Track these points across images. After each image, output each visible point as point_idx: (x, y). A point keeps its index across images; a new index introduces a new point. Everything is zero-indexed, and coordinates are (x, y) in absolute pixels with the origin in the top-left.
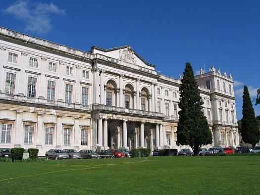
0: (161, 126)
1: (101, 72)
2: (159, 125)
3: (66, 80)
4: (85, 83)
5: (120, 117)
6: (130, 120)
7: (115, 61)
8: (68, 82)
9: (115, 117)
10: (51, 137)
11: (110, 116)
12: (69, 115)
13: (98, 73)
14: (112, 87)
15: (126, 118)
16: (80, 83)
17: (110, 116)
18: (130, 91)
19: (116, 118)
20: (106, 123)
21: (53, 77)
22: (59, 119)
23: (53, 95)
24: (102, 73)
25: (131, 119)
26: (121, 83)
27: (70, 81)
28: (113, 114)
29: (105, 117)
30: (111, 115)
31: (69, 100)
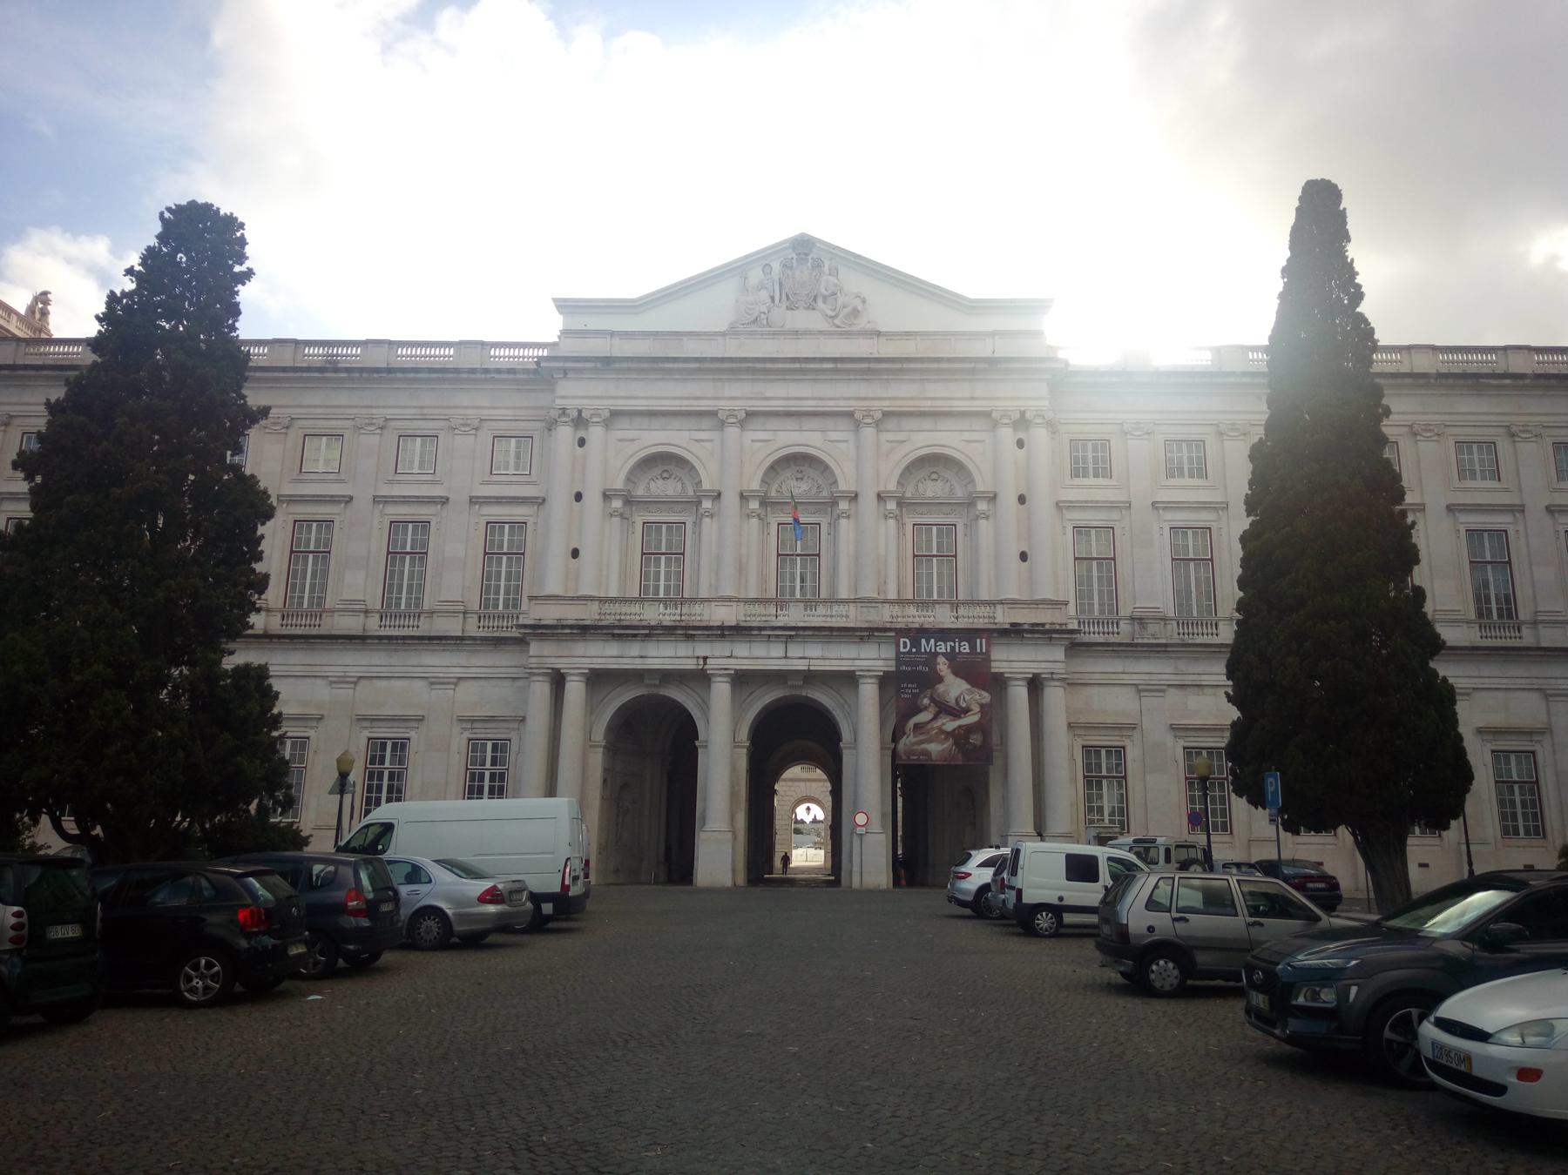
0: (1054, 697)
1: (580, 421)
2: (1035, 685)
13: (565, 433)
16: (474, 501)
20: (575, 690)
24: (595, 434)
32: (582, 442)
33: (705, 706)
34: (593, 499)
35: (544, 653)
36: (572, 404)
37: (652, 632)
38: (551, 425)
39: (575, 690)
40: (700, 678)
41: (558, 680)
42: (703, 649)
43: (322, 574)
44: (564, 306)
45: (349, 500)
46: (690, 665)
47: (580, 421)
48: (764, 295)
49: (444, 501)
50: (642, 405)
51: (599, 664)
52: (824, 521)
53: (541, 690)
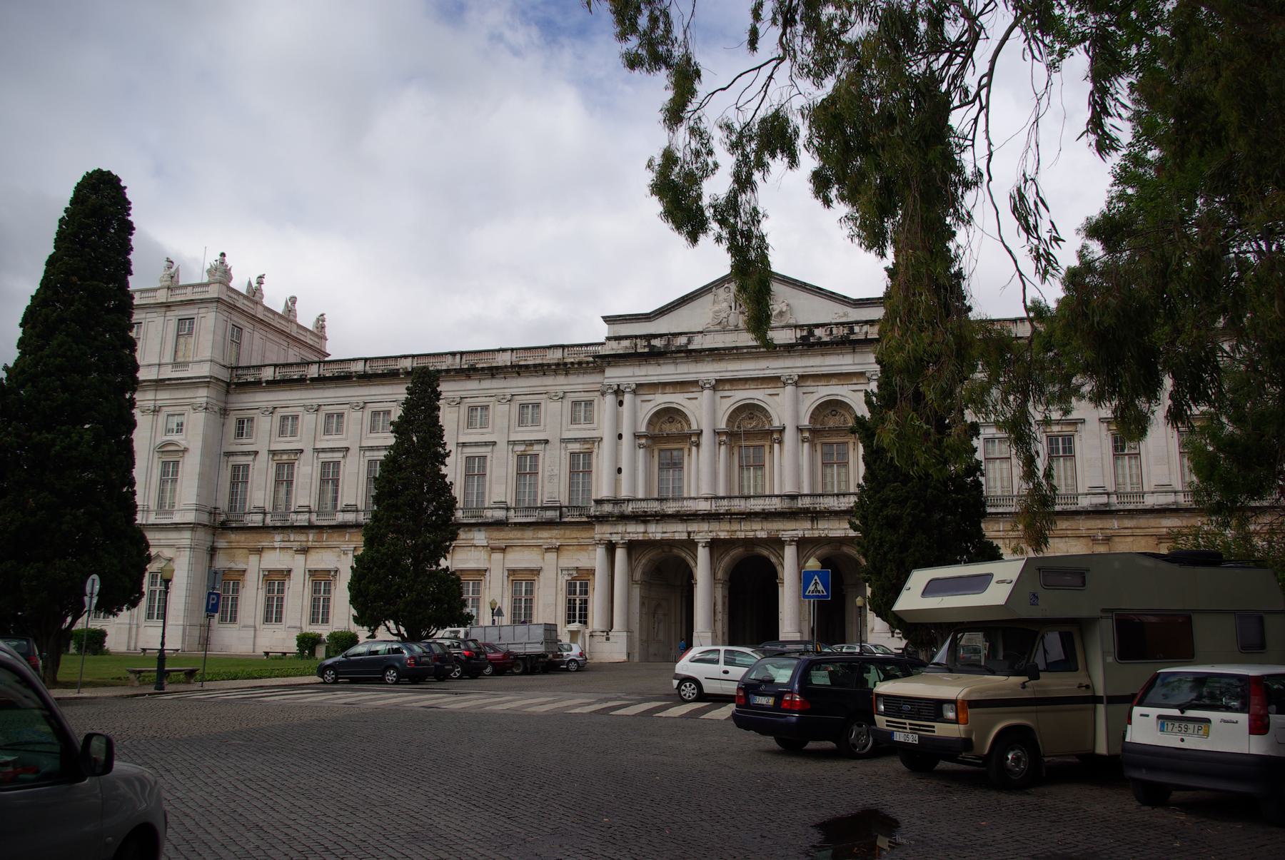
1: (618, 392)
3: (514, 443)
4: (576, 440)
5: (677, 531)
6: (723, 535)
7: (682, 340)
8: (522, 448)
9: (656, 532)
10: (280, 606)
11: (635, 531)
12: (525, 542)
13: (610, 399)
14: (666, 436)
15: (703, 532)
16: (563, 441)
17: (635, 531)
18: (748, 432)
19: (658, 537)
20: (620, 554)
21: (477, 444)
22: (497, 556)
23: (481, 495)
24: (627, 398)
25: (722, 531)
26: (705, 412)
27: (531, 443)
28: (645, 522)
29: (615, 538)
30: (641, 528)
31: (517, 501)
32: (621, 403)
33: (695, 558)
34: (627, 437)
35: (603, 532)
36: (614, 382)
37: (662, 517)
38: (603, 394)
39: (620, 554)
40: (691, 544)
41: (611, 548)
42: (693, 527)
43: (482, 485)
44: (609, 320)
45: (494, 443)
46: (684, 536)
47: (618, 392)
48: (725, 305)
49: (546, 442)
50: (655, 379)
51: (635, 537)
52: (767, 444)
53: (600, 552)
